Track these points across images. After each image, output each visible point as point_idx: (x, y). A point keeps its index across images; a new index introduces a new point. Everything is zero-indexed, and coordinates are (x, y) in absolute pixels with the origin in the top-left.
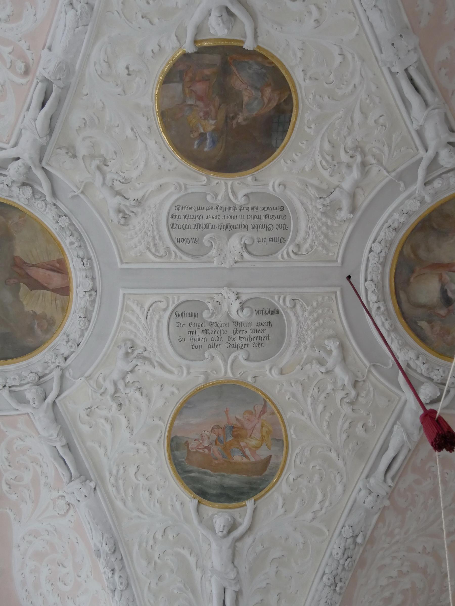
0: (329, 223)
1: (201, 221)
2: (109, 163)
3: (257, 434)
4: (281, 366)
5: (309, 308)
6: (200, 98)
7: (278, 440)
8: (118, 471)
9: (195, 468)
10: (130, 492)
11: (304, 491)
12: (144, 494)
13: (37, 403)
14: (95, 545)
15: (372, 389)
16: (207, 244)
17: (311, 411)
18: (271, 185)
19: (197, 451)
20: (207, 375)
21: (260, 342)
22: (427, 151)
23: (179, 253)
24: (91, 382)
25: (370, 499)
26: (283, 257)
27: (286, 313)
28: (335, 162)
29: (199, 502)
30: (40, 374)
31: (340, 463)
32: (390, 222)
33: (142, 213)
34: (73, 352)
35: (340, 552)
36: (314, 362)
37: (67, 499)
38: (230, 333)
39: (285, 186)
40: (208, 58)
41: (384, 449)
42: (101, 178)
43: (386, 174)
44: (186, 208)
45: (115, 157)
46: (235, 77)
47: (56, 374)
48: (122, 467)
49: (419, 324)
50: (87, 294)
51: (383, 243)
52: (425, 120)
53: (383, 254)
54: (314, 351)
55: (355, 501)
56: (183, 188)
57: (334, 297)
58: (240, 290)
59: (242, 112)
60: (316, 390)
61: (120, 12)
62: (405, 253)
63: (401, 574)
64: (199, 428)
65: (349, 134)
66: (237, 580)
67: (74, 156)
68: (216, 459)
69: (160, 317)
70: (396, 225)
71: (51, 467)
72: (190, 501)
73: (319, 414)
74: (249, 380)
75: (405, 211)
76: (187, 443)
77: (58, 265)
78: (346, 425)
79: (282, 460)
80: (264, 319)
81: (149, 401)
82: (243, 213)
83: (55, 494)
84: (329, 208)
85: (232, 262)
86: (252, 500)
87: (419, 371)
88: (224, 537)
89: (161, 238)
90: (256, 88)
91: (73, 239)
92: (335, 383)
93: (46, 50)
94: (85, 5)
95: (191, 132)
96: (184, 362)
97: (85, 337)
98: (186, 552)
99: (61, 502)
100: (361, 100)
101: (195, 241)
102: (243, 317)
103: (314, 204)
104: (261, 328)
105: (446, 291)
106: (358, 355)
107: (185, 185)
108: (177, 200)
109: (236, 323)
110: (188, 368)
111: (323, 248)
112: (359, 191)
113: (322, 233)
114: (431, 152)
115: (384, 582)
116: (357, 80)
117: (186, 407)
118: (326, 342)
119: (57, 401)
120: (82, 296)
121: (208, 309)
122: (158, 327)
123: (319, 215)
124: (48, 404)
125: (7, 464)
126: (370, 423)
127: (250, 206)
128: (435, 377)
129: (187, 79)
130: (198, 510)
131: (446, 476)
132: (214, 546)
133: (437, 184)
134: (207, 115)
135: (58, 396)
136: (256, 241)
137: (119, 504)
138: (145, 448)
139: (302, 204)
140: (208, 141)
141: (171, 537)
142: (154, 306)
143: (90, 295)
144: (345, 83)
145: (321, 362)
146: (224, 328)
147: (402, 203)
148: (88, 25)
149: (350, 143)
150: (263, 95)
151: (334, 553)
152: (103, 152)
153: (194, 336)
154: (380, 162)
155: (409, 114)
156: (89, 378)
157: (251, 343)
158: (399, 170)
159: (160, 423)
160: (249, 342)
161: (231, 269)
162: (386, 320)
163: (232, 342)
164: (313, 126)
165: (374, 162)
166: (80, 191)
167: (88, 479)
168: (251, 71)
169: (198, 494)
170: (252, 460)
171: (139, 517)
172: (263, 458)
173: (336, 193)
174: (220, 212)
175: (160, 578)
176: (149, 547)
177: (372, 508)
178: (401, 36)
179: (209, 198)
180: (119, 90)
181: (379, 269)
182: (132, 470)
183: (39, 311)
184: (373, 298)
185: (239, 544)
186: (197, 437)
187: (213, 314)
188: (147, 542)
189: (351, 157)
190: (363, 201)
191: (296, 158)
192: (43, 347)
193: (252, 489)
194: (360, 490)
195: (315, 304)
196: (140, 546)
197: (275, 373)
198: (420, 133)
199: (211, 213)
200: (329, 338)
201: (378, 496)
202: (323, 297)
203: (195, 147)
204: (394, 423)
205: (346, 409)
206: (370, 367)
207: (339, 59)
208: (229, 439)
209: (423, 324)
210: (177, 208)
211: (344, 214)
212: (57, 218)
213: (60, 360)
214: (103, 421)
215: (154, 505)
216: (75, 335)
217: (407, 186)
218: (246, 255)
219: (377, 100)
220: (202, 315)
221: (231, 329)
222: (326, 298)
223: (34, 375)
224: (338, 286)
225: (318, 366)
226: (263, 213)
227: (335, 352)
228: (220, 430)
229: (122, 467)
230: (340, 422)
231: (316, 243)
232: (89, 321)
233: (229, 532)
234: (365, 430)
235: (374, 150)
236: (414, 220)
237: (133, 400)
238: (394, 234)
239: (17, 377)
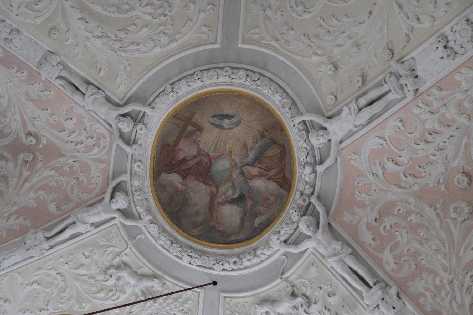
15: (301, 280)
22: (116, 218)
28: (114, 289)
49: (257, 225)
52: (85, 223)
53: (193, 255)
57: (228, 300)
62: (198, 233)
65: (94, 277)
70: (169, 243)
87: (291, 232)
100: (70, 269)
103: (147, 308)
105: (233, 199)
106: (273, 288)
111: (186, 303)
112: (140, 271)
113: (172, 303)
116: (53, 273)
123: (156, 305)
126: (330, 290)
131: (401, 212)
144: (54, 281)
149: (100, 278)
154: (119, 254)
158: (126, 239)
164: (84, 305)
165: (118, 259)
177: (394, 308)
181: (204, 259)
189: (111, 277)
198: (96, 225)
201: (383, 299)
202: (227, 309)
206: (281, 278)
207: (35, 286)
209: (258, 221)
217: (142, 233)
219: (71, 257)
222: (228, 306)
231: (182, 308)
234: (334, 295)
238: (175, 245)
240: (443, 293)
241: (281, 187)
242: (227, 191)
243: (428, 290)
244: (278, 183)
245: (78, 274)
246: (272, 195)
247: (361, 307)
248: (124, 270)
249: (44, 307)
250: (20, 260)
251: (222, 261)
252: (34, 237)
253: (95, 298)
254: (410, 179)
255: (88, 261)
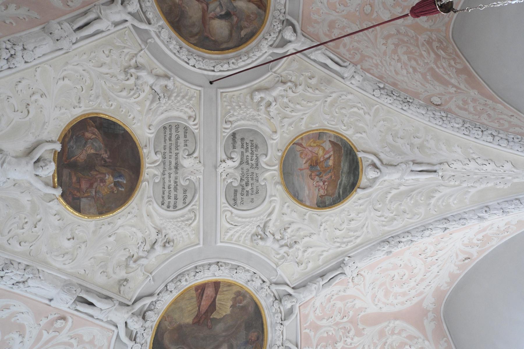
0: (175, 95)
1: (172, 187)
2: (132, 254)
3: (316, 150)
4: (271, 133)
5: (232, 112)
6: (91, 186)
7: (319, 136)
8: (338, 242)
9: (337, 191)
10: (351, 234)
11: (352, 120)
12: (353, 225)
13: (294, 300)
14: (384, 255)
15: (286, 72)
16: (187, 183)
17: (300, 113)
18: (150, 135)
19: (326, 190)
20: (276, 183)
21: (255, 146)
22: (126, 21)
23: (193, 203)
24: (280, 263)
25: (357, 77)
26: (197, 129)
27: (235, 128)
28: (135, 88)
29: (359, 188)
30: (274, 299)
31: (334, 95)
32: (176, 52)
33: (166, 230)
34: (260, 277)
35: (389, 98)
36: (269, 109)
37: (355, 275)
38: (248, 167)
39: (150, 125)
40: (65, 178)
41: (325, 66)
42: (143, 259)
43: (142, 52)
44: (163, 197)
45: (128, 250)
46: (78, 159)
47: (274, 288)
48: (336, 240)
50: (221, 268)
51: (189, 57)
52: (109, 21)
53: (197, 58)
54: (261, 109)
55: (358, 87)
56: (149, 199)
57: (224, 94)
58: (219, 160)
59: (101, 155)
60: (287, 109)
61: (31, 244)
62: (195, 42)
63: (399, 60)
64: (311, 188)
66: (406, 163)
67: (126, 280)
68: (331, 177)
69: (236, 216)
70: (178, 47)
71: (334, 288)
72: (358, 194)
73: (302, 108)
74: (280, 154)
75: (169, 40)
76: (321, 196)
77: (199, 291)
78: (309, 89)
79: (332, 133)
80: (239, 143)
81: (293, 222)
82: (167, 156)
83: (351, 284)
84: (166, 94)
85: (200, 165)
86: (358, 153)
87: (275, 39)
88: (381, 171)
89: (183, 216)
90: (86, 143)
91: (183, 279)
92: (282, 96)
93: (52, 303)
94: (26, 271)
95: (113, 192)
96: (267, 199)
97: (249, 269)
98: (389, 196)
99: (356, 280)
100: (93, 66)
101: (185, 191)
102: (237, 157)
104: (245, 145)
105: (221, 15)
106: (263, 80)
107: (148, 198)
108: (158, 204)
109: (241, 163)
110: (271, 196)
111: (191, 100)
113: (181, 100)
114: (128, 18)
115: (404, 72)
116: (80, 69)
117: (298, 197)
118: (255, 101)
119: (292, 286)
120: (222, 272)
121: (231, 182)
122: (243, 218)
123: (170, 102)
124: (295, 292)
125: (331, 319)
126: (309, 74)
127: (163, 151)
128: (279, 29)
129: (78, 194)
130: (364, 189)
132: (386, 178)
133: (150, 16)
134: (103, 181)
135: (288, 285)
136: (186, 147)
137: (358, 241)
138: (324, 224)
139: (162, 113)
140: (120, 180)
141: (380, 206)
142: (229, 221)
143: (221, 266)
145: (269, 105)
146: (245, 171)
147: (163, 42)
148: (38, 270)
149: (122, 77)
150: (90, 139)
151: (390, 102)
152: (124, 259)
153: (250, 192)
155: (102, 32)
156: (277, 265)
157: (255, 153)
159: (308, 214)
160: (255, 154)
161: (204, 165)
162: (241, 58)
163: (255, 166)
164: (110, 103)
166: (150, 275)
167: (343, 262)
168: (75, 146)
169: (353, 189)
170: (332, 153)
171: (367, 227)
172: (331, 146)
173: (157, 88)
174: (166, 173)
175: (405, 212)
176: (386, 220)
178: (51, 33)
179: (157, 181)
180: (83, 246)
182: (338, 233)
183: (230, 303)
184: (226, 67)
185: (385, 162)
186: (317, 190)
187: (235, 179)
188: (383, 221)
190: (161, 69)
191: (132, 116)
192: (255, 299)
193: (350, 154)
194: (351, 83)
195: (229, 107)
196: (385, 226)
197: (275, 137)
198: (116, 24)
199: (167, 180)
200: (252, 99)
203: (123, 190)
204: (309, 58)
205: (300, 89)
208: (319, 169)
210: (163, 204)
211: (170, 84)
212: (169, 292)
213: (265, 286)
214: (306, 254)
215: (360, 217)
216: (248, 276)
217: (151, 37)
218: (195, 155)
220: (235, 187)
221: (245, 166)
222: (225, 99)
223: (275, 303)
224: (217, 90)
225: (271, 107)
226: (168, 142)
227: (262, 95)
228: (313, 174)
229: (336, 240)
230: (308, 94)
232: (239, 266)
233: (377, 168)
235: (126, 59)
236: (174, 34)
237: (292, 234)
239: (276, 315)
240: (379, 66)
241: (259, 8)
242: (216, 9)
243: (372, 66)
244: (256, 5)
245: (101, 73)
246: (252, 13)
247: (335, 80)
248: (144, 69)
249: (77, 104)
250: (49, 51)
251: (221, 63)
252: (60, 28)
253: (118, 96)
254: (342, 6)
255: (108, 60)
